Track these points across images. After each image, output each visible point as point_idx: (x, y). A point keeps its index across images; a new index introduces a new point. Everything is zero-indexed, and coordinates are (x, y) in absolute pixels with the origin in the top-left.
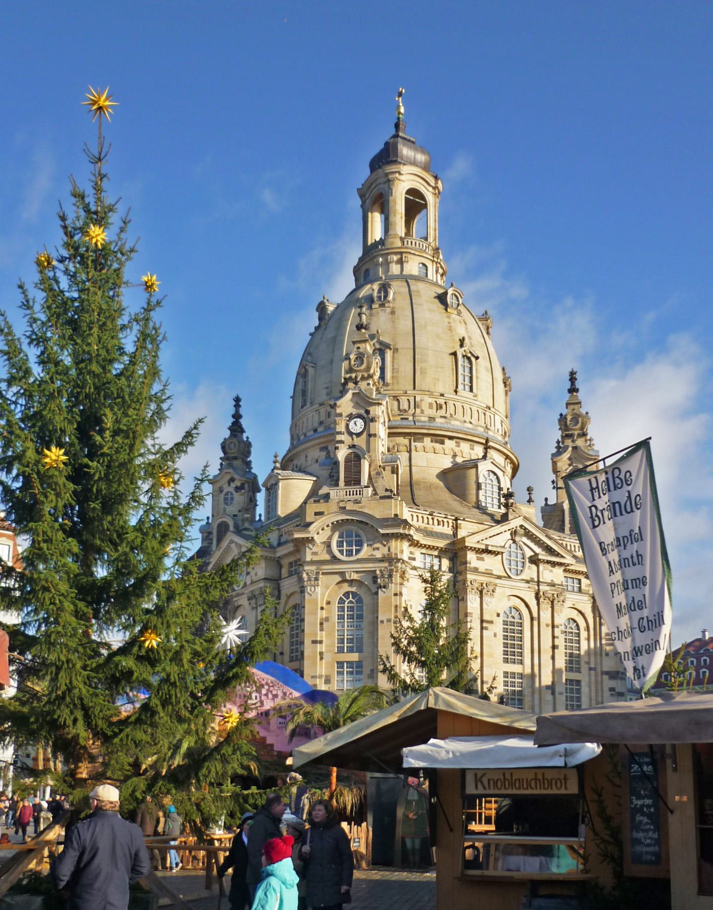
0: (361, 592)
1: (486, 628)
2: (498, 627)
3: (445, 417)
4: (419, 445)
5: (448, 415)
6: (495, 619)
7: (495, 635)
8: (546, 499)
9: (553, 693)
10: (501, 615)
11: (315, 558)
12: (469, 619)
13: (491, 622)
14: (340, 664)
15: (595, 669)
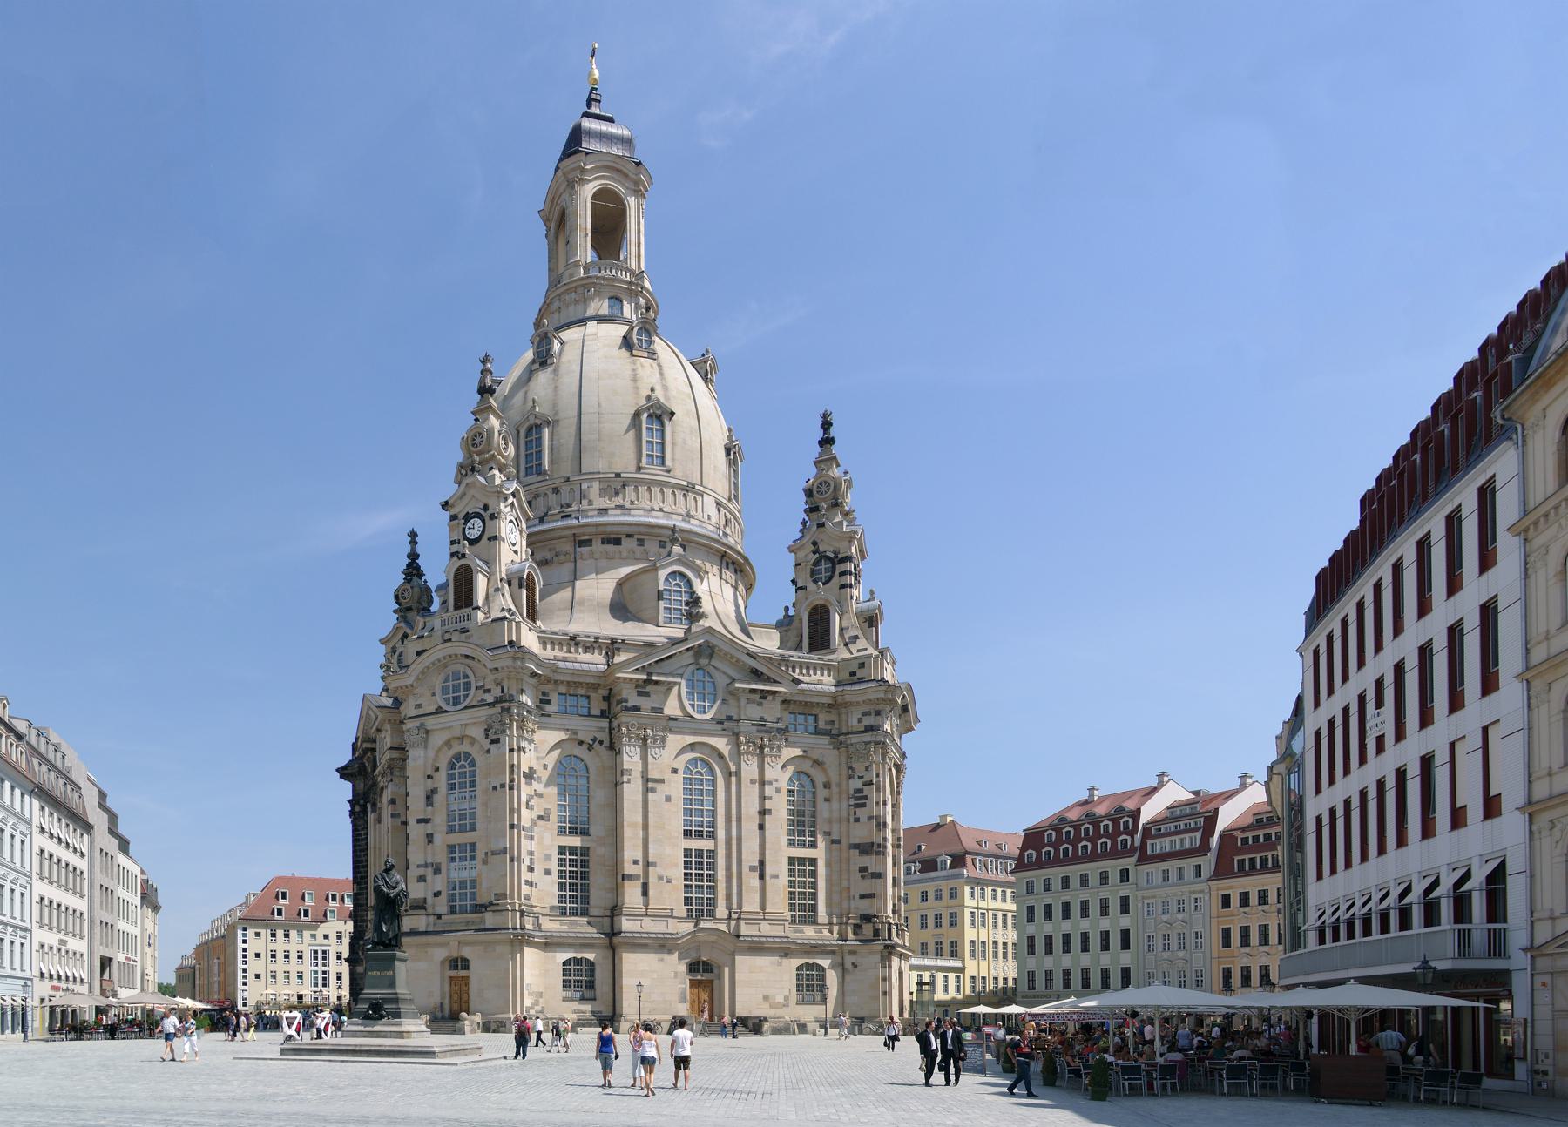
0: (474, 752)
1: (653, 790)
2: (675, 786)
3: (621, 507)
4: (585, 550)
5: (628, 505)
6: (668, 776)
7: (668, 799)
8: (787, 609)
9: (762, 876)
10: (681, 772)
11: (420, 712)
12: (625, 778)
13: (662, 781)
14: (452, 849)
15: (838, 842)
